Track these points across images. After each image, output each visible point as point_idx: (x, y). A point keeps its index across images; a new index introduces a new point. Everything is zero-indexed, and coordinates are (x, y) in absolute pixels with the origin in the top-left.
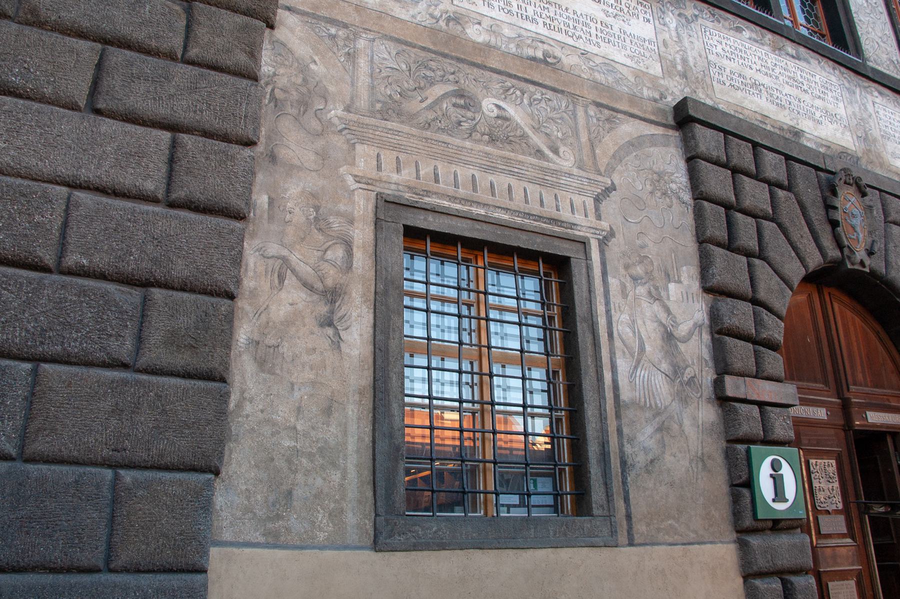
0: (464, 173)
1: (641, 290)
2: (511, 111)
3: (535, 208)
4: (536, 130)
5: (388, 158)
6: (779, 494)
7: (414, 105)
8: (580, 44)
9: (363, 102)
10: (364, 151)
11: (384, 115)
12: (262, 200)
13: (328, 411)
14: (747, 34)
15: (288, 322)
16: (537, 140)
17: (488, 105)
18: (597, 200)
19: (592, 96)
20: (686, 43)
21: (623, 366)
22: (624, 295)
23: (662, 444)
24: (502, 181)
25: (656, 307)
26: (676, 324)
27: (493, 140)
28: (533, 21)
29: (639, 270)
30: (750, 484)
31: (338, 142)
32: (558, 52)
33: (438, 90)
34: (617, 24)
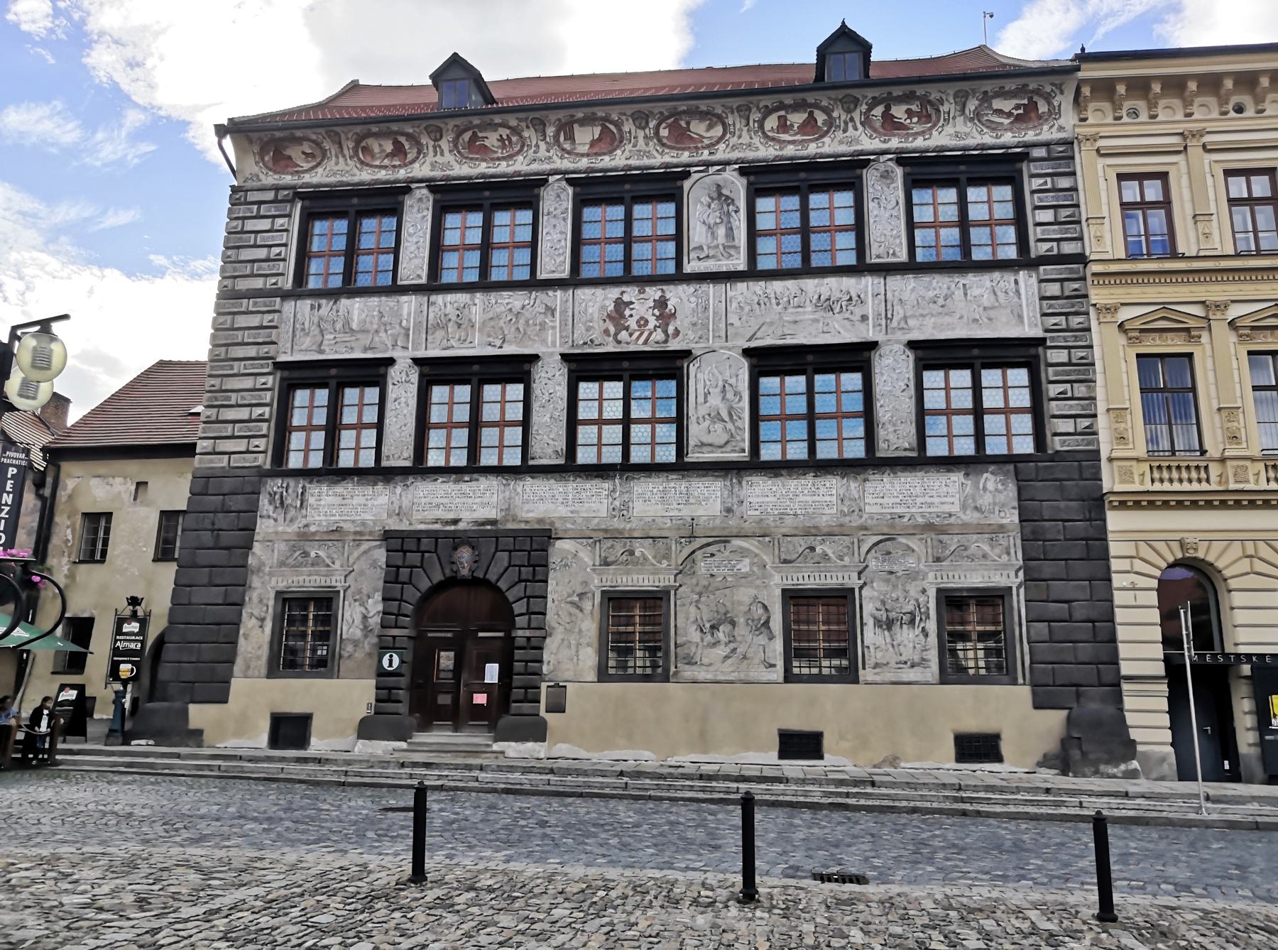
0: (301, 579)
1: (357, 603)
2: (321, 553)
3: (323, 584)
4: (328, 557)
5: (280, 579)
6: (390, 665)
7: (290, 561)
8: (352, 518)
9: (275, 565)
10: (274, 579)
11: (281, 567)
12: (247, 599)
13: (259, 648)
14: (440, 480)
15: (253, 627)
16: (328, 561)
17: (313, 554)
18: (346, 576)
19: (351, 537)
20: (403, 498)
21: (345, 628)
22: (350, 606)
23: (355, 651)
24: (313, 578)
25: (362, 609)
26: (368, 612)
27: (313, 565)
28: (335, 515)
29: (357, 597)
30: (380, 661)
31: (267, 578)
32: (342, 524)
33: (297, 553)
34: (370, 503)
